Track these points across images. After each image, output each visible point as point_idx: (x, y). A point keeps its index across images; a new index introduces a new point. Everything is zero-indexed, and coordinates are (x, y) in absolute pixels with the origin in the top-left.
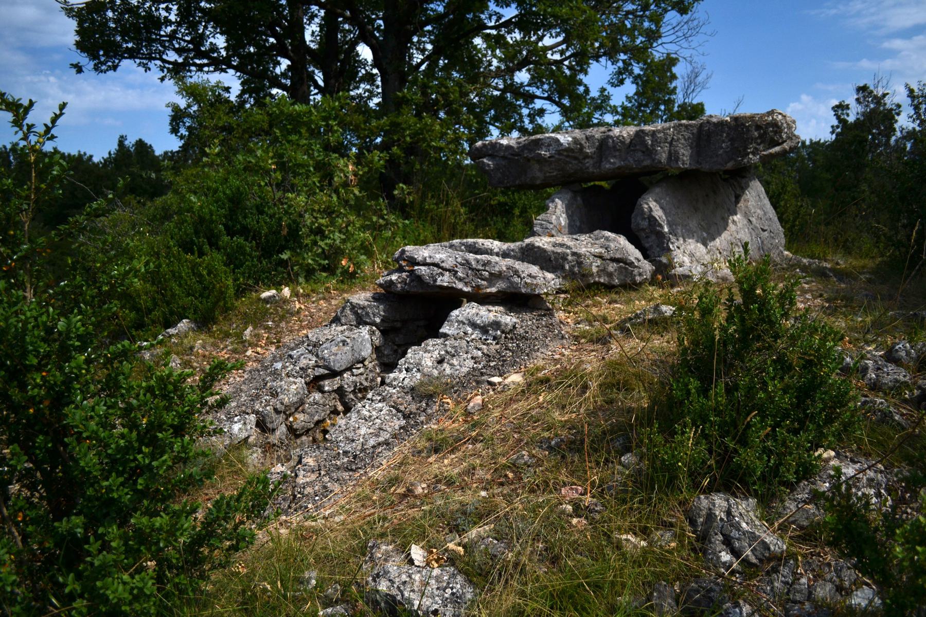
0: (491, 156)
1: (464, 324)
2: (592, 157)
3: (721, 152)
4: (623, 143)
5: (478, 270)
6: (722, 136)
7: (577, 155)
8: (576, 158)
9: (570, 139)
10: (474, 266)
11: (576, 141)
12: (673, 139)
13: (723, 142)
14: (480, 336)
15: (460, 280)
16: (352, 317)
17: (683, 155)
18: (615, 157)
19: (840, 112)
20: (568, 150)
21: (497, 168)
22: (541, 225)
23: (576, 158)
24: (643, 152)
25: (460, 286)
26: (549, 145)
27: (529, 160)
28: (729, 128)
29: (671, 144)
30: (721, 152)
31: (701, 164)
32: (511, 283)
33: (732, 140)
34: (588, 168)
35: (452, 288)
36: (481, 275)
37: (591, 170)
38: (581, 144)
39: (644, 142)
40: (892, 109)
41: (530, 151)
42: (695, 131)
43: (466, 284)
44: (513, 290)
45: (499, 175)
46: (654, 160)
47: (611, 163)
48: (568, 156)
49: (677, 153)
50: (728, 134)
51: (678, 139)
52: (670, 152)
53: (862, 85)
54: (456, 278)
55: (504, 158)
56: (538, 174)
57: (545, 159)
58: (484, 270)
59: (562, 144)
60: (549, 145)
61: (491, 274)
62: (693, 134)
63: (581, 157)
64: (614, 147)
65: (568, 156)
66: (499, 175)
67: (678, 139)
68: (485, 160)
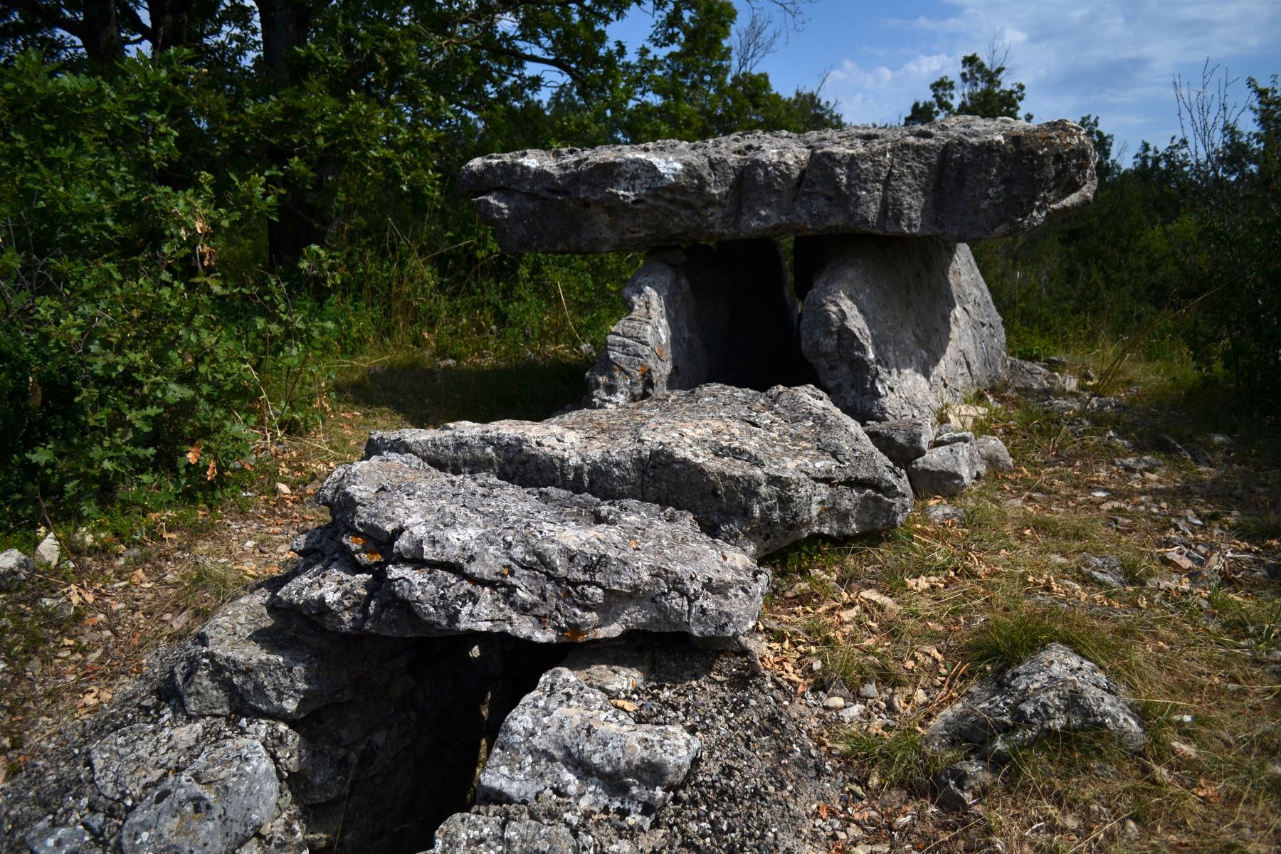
0: (504, 192)
1: (552, 759)
2: (720, 204)
3: (985, 204)
4: (786, 177)
5: (575, 584)
6: (988, 172)
7: (691, 199)
8: (687, 206)
9: (679, 166)
10: (562, 571)
11: (690, 169)
12: (890, 173)
13: (991, 185)
14: (603, 800)
15: (524, 609)
16: (216, 694)
17: (911, 208)
18: (769, 205)
19: (941, 92)
20: (675, 188)
21: (517, 215)
22: (624, 346)
23: (687, 206)
24: (829, 199)
25: (524, 628)
26: (634, 177)
27: (586, 204)
28: (1003, 157)
29: (886, 184)
30: (985, 204)
31: (942, 226)
32: (663, 611)
33: (1005, 181)
34: (712, 225)
35: (504, 634)
36: (583, 596)
37: (718, 229)
38: (700, 177)
39: (832, 179)
40: (1012, 92)
41: (593, 187)
42: (934, 160)
43: (541, 621)
45: (521, 230)
46: (852, 216)
47: (761, 218)
48: (671, 201)
49: (897, 203)
50: (1000, 170)
51: (902, 175)
52: (884, 200)
53: (969, 55)
54: (513, 604)
55: (531, 196)
57: (624, 204)
58: (590, 584)
59: (661, 177)
60: (634, 177)
61: (608, 592)
62: (929, 165)
63: (699, 204)
65: (671, 201)
66: (521, 230)
67: (902, 175)
68: (491, 200)
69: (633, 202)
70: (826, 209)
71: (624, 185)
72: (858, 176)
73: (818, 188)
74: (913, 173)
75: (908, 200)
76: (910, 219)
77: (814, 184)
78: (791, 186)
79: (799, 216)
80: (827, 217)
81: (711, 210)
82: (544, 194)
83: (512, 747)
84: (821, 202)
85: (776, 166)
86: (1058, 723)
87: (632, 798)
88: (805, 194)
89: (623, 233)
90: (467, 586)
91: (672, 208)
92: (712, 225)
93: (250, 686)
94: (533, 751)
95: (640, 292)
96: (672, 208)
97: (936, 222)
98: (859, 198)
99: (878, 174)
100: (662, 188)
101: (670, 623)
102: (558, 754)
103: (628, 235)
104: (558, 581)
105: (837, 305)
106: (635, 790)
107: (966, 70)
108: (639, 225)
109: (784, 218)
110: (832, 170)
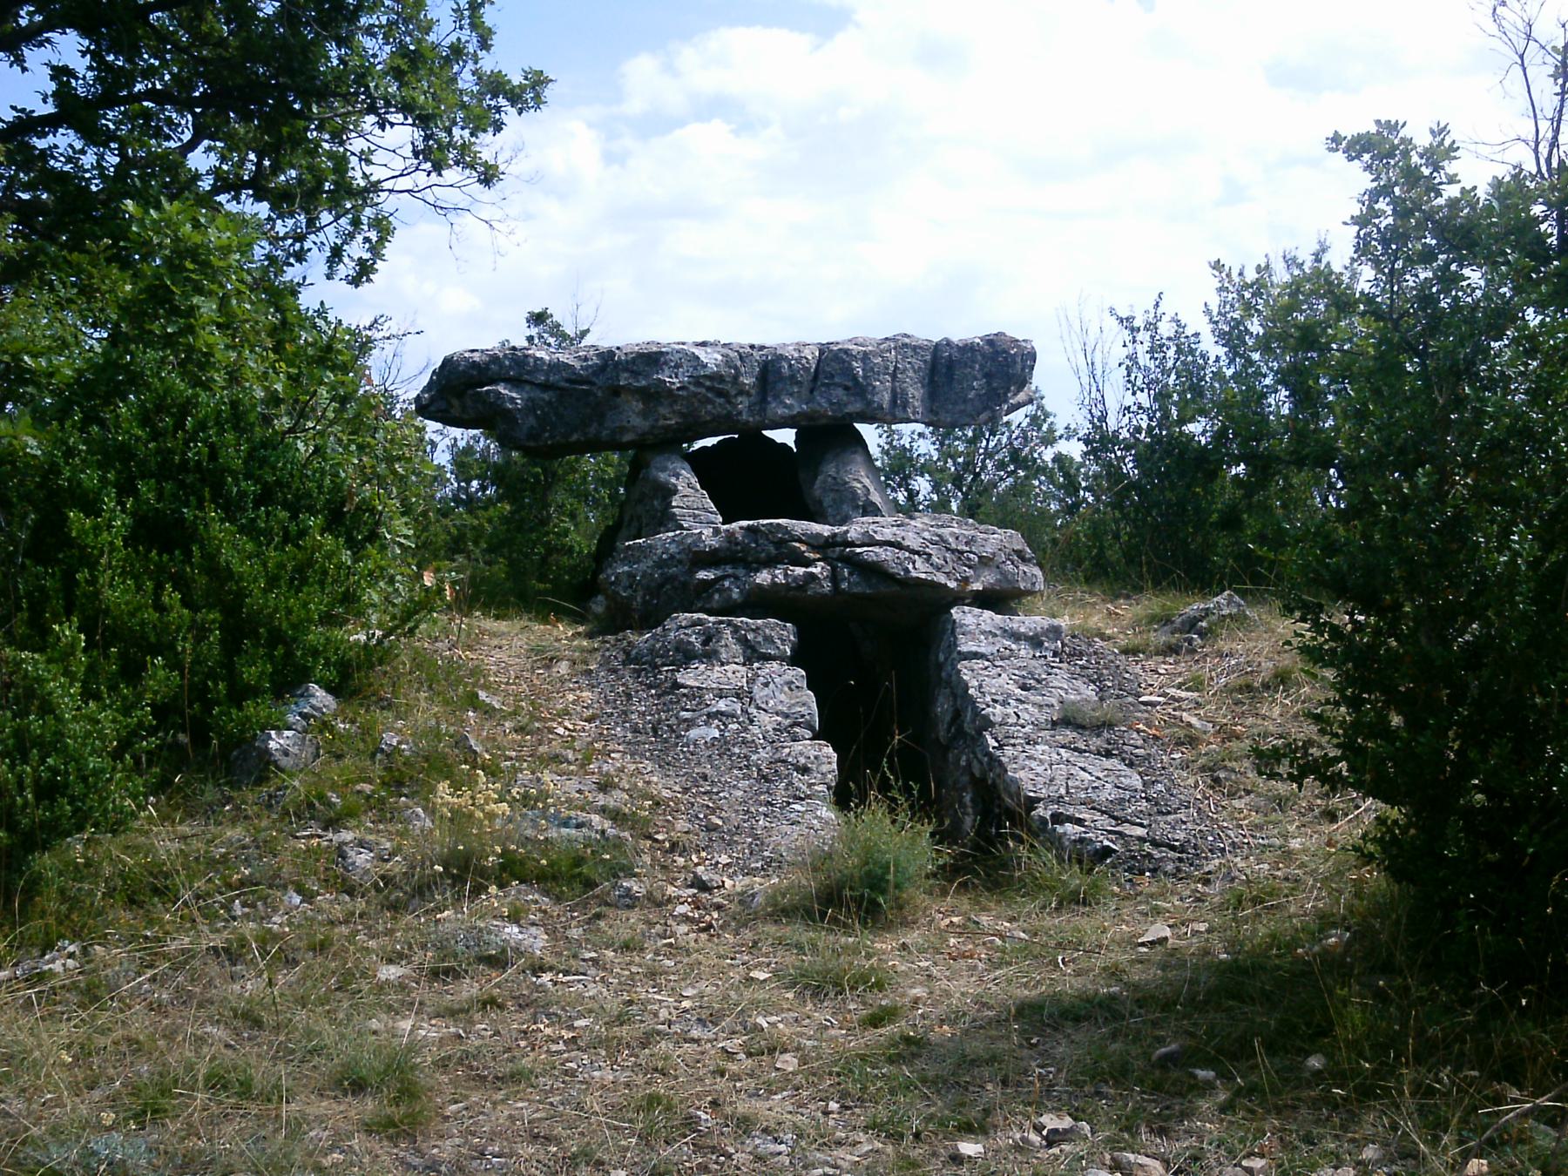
0: (515, 383)
1: (995, 635)
2: (748, 394)
3: (971, 395)
4: (807, 370)
5: (962, 553)
6: (972, 368)
7: (728, 387)
8: (720, 393)
9: (720, 358)
10: (954, 546)
12: (896, 368)
15: (938, 569)
16: (736, 648)
18: (791, 395)
20: (716, 377)
21: (531, 406)
22: (695, 516)
23: (720, 393)
24: (846, 388)
25: (941, 578)
26: (678, 366)
27: (616, 391)
28: (983, 356)
29: (894, 376)
30: (971, 395)
31: (937, 414)
33: (986, 375)
34: (740, 413)
35: (932, 581)
36: (969, 559)
38: (736, 368)
39: (848, 372)
41: (636, 374)
42: (928, 358)
44: (1005, 585)
45: (532, 421)
46: (869, 403)
47: (786, 406)
48: (709, 389)
49: (904, 392)
50: (982, 368)
51: (905, 369)
52: (894, 391)
53: (537, 311)
55: (545, 387)
56: (636, 421)
57: (670, 391)
58: (971, 552)
59: (705, 366)
60: (678, 366)
62: (925, 361)
63: (733, 392)
64: (792, 377)
65: (709, 389)
66: (532, 421)
68: (502, 389)
69: (678, 389)
70: (845, 398)
71: (667, 372)
72: (872, 369)
73: (837, 380)
74: (913, 368)
75: (911, 391)
76: (914, 407)
77: (832, 376)
78: (810, 378)
79: (819, 404)
80: (845, 405)
81: (740, 399)
82: (563, 384)
83: (970, 632)
84: (840, 392)
85: (798, 360)
86: (1225, 612)
87: (1047, 649)
88: (824, 385)
89: (657, 420)
90: (907, 554)
91: (709, 395)
92: (740, 413)
93: (760, 639)
94: (983, 632)
95: (677, 476)
96: (709, 395)
97: (932, 411)
98: (874, 387)
99: (887, 368)
100: (705, 376)
101: (1008, 581)
102: (998, 632)
103: (661, 422)
104: (953, 551)
105: (861, 482)
106: (1046, 644)
107: (534, 331)
108: (674, 412)
109: (805, 407)
110: (850, 364)
